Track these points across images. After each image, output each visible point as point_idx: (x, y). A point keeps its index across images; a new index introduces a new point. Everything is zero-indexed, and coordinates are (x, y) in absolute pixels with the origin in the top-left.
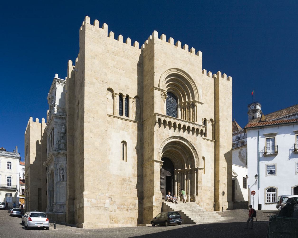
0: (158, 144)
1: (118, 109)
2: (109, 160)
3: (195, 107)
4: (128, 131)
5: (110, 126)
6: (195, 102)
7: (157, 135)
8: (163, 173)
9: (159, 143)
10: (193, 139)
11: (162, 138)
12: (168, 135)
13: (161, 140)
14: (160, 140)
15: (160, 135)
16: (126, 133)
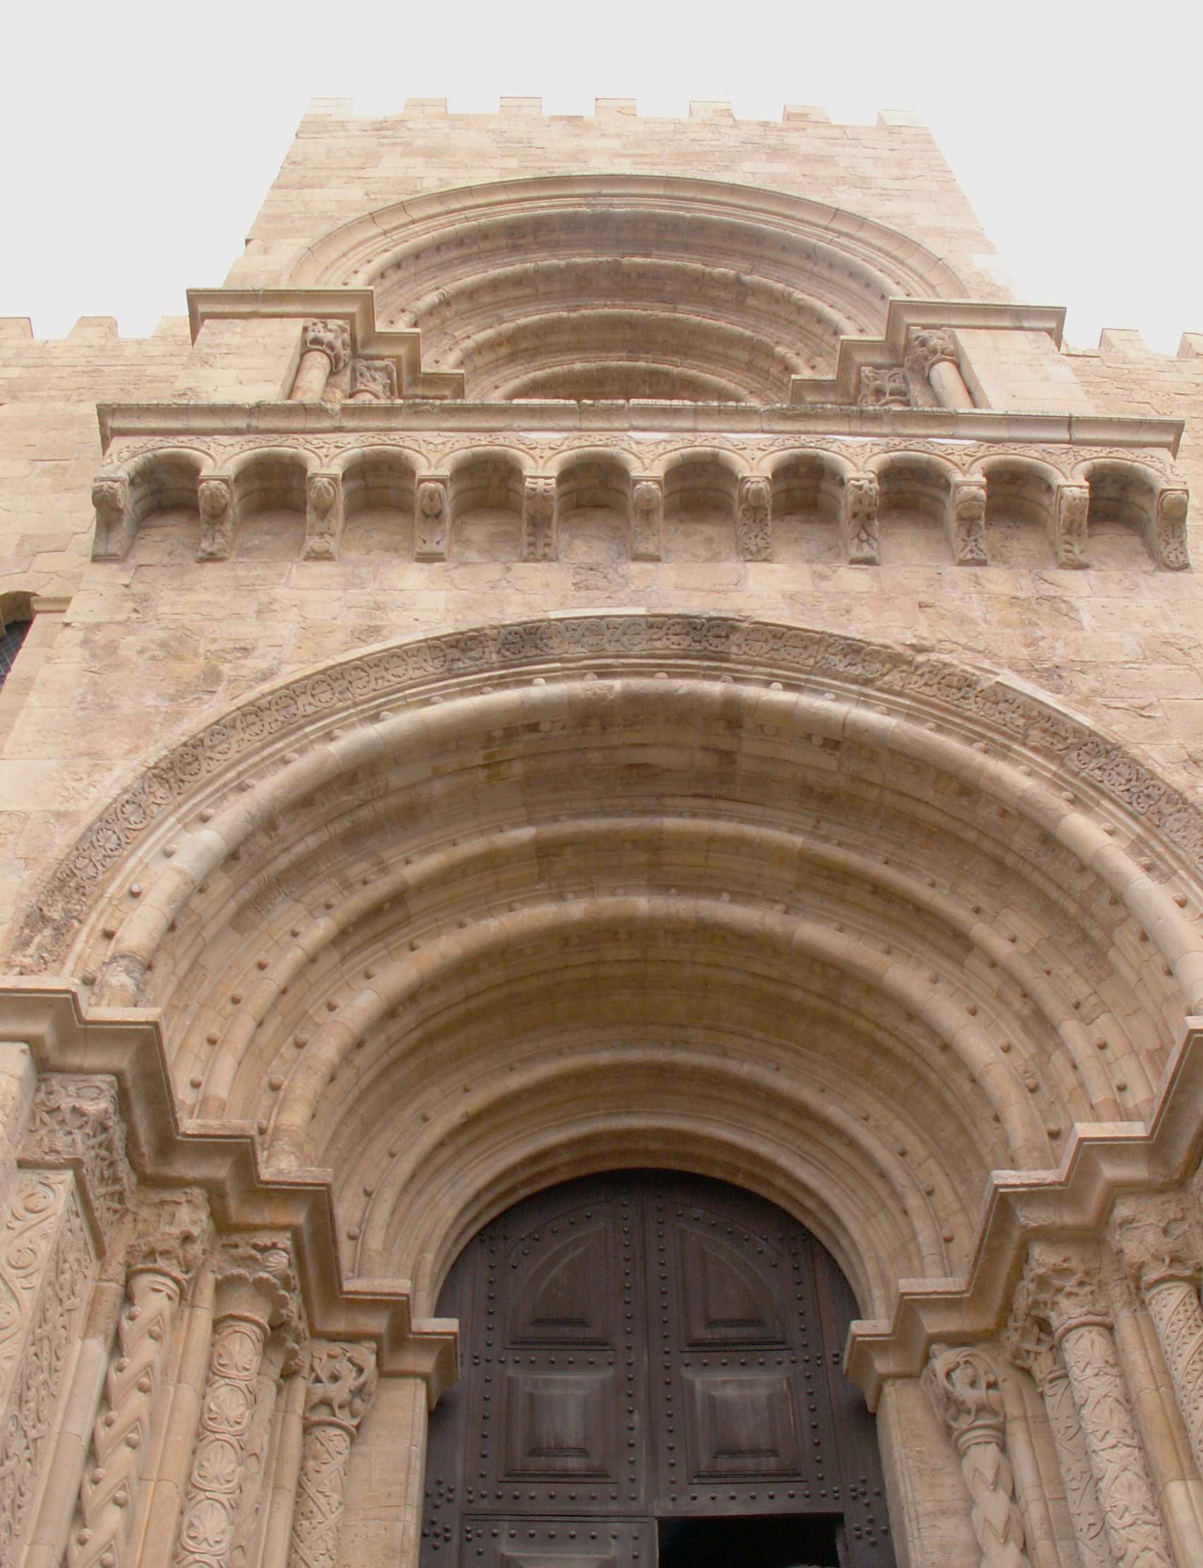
3: (944, 373)
6: (909, 319)
8: (567, 1476)
10: (977, 614)
11: (212, 677)
14: (150, 700)
15: (173, 649)
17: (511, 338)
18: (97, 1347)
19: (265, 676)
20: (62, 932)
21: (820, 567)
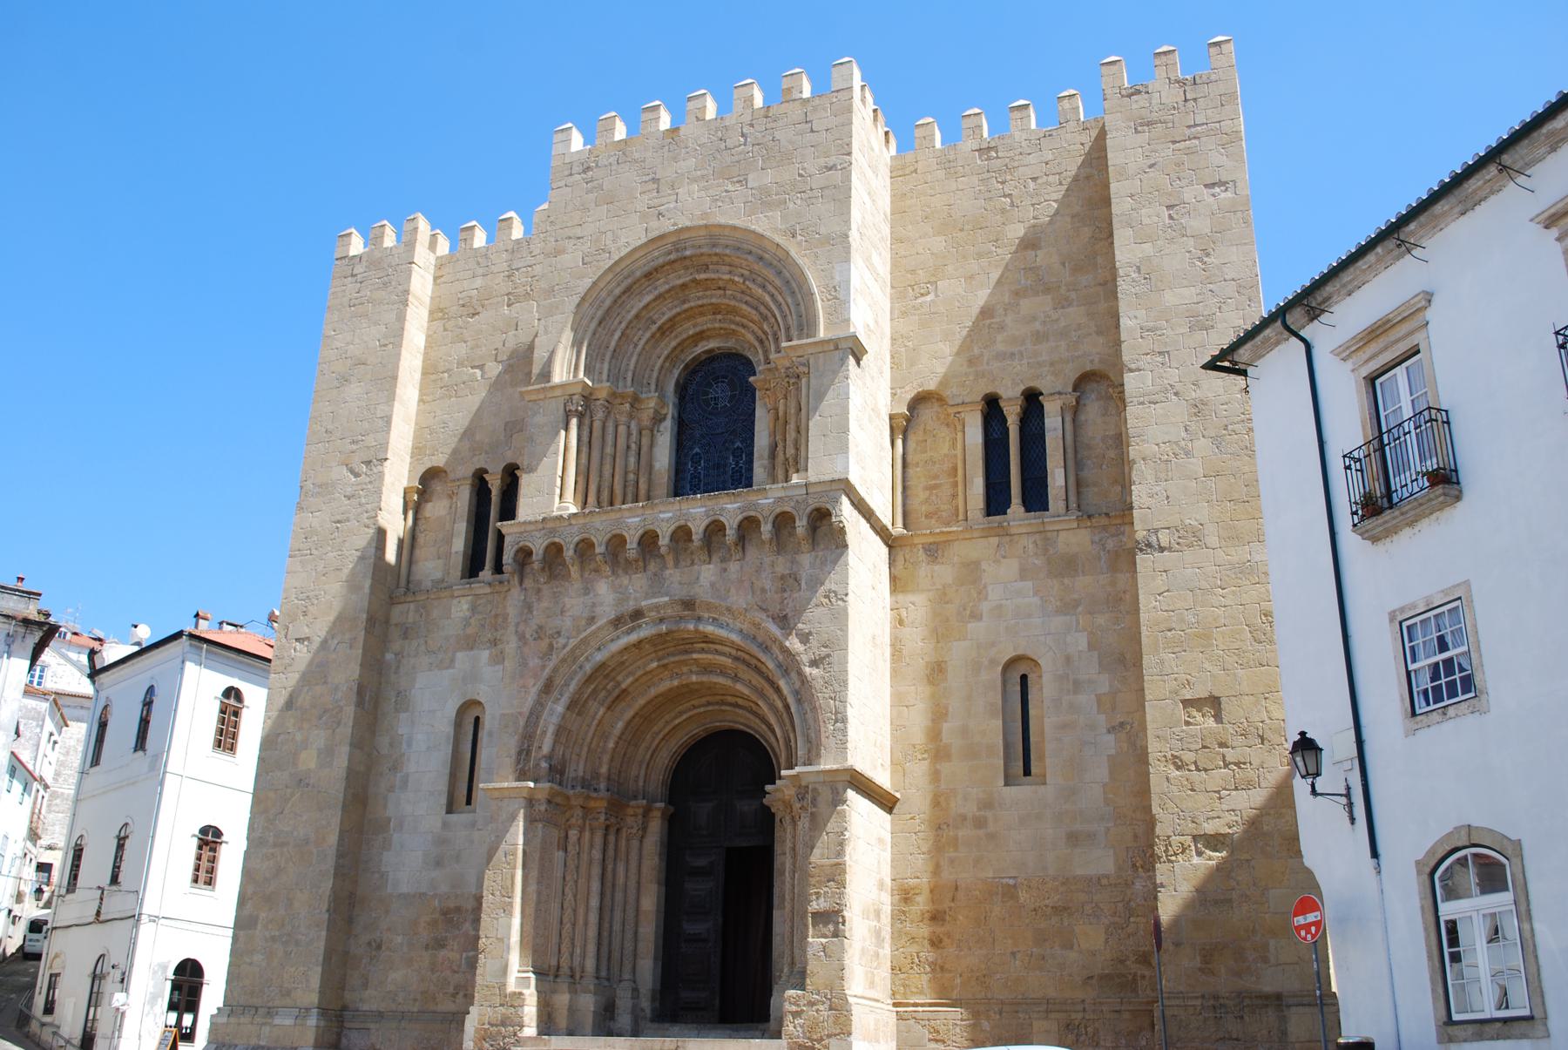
0: (524, 686)
1: (456, 553)
2: (389, 820)
4: (495, 643)
5: (414, 643)
7: (522, 637)
9: (532, 681)
10: (767, 587)
11: (551, 647)
12: (593, 618)
13: (542, 659)
14: (537, 661)
16: (485, 655)
17: (660, 328)
18: (561, 853)
19: (564, 646)
20: (528, 752)
21: (724, 565)
